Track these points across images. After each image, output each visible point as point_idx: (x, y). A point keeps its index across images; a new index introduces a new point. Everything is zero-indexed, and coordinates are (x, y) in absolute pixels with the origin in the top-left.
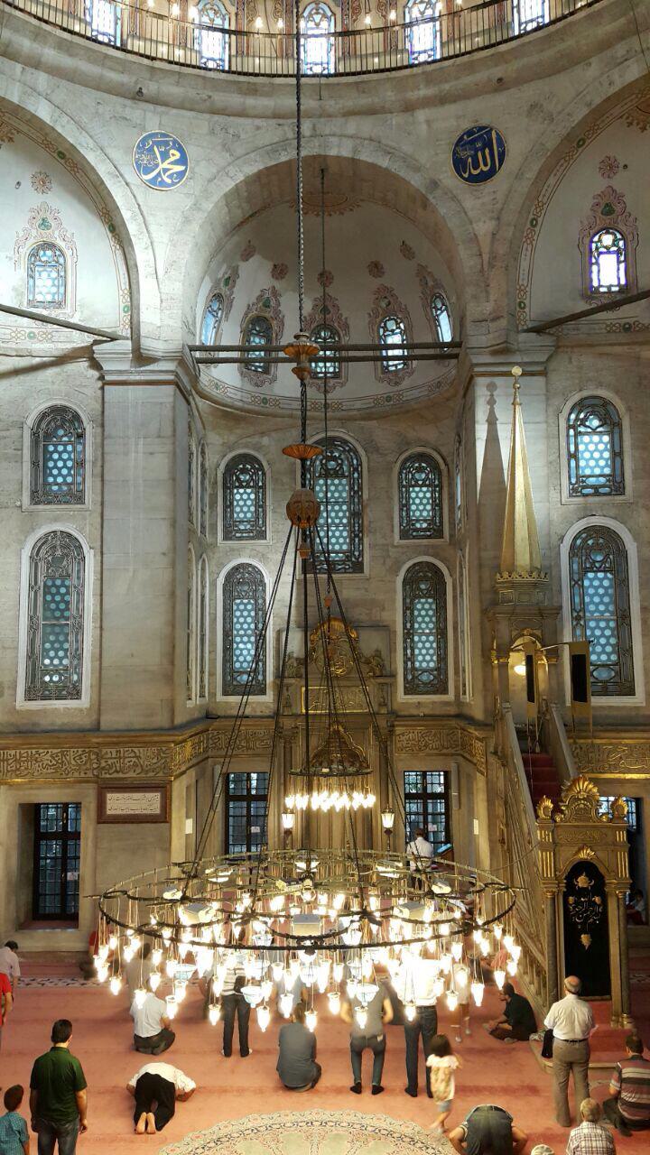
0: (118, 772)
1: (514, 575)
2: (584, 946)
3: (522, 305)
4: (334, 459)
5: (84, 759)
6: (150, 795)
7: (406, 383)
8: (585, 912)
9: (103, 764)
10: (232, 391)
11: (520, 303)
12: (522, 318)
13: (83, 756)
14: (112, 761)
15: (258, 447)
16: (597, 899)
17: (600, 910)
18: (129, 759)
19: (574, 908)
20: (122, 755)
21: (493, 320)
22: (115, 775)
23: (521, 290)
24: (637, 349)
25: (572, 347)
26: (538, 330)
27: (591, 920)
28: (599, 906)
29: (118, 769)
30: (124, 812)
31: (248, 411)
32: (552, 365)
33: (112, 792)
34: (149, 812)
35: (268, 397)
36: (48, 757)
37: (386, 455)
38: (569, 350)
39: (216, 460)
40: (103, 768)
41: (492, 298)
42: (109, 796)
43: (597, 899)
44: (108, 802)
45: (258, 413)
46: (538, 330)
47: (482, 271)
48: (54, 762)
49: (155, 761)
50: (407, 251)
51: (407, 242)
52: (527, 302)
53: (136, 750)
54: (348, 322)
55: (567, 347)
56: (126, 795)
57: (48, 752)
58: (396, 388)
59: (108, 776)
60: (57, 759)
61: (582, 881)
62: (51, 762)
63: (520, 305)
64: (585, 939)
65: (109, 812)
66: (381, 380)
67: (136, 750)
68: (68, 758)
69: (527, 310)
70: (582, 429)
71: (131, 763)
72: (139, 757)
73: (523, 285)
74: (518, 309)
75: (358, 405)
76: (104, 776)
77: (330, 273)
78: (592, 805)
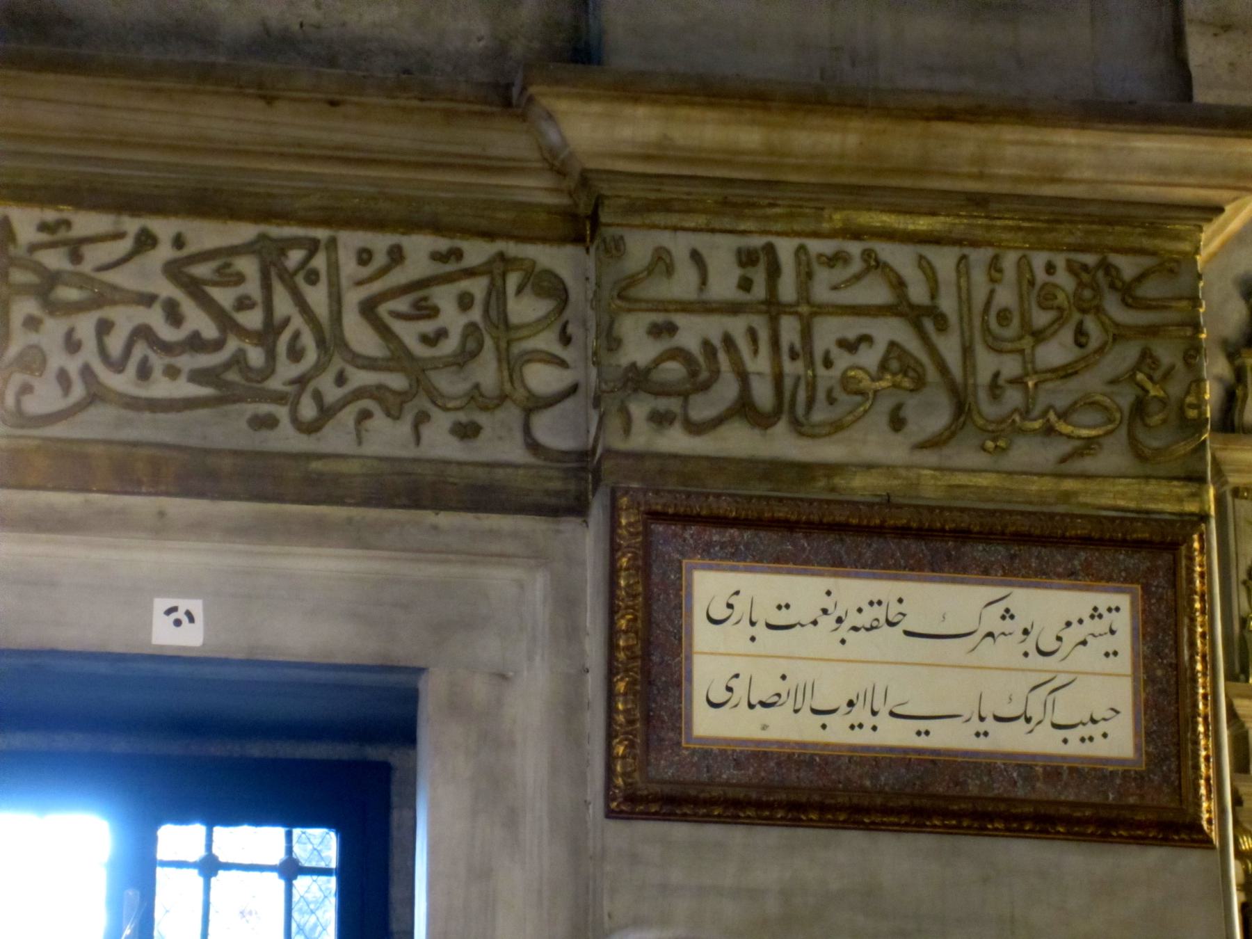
0: (761, 420)
5: (452, 319)
6: (1049, 607)
9: (638, 349)
13: (445, 297)
14: (713, 327)
18: (852, 328)
20: (787, 290)
22: (739, 441)
29: (763, 394)
30: (838, 733)
33: (736, 557)
34: (1042, 742)
36: (148, 275)
40: (638, 380)
42: (710, 587)
44: (703, 636)
48: (198, 321)
49: (1056, 352)
53: (899, 257)
56: (854, 591)
57: (146, 241)
59: (676, 441)
60: (224, 297)
62: (174, 315)
65: (707, 724)
67: (899, 257)
68: (317, 297)
71: (870, 358)
72: (922, 317)
76: (642, 438)
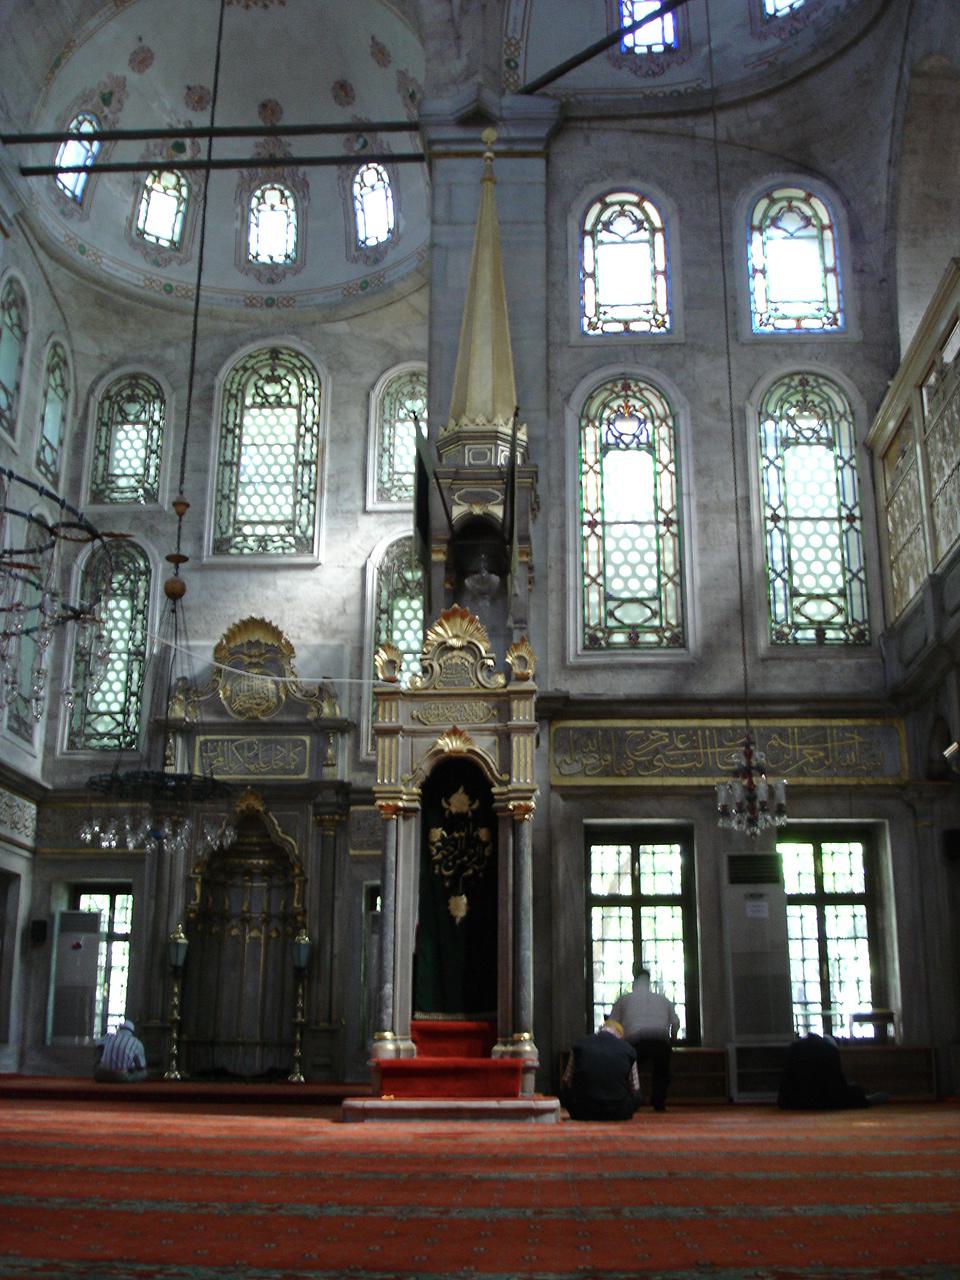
1: (464, 420)
2: (453, 919)
3: (512, 64)
4: (276, 380)
7: (390, 258)
8: (460, 856)
10: (111, 264)
11: (508, 62)
12: (511, 80)
15: (158, 364)
16: (483, 834)
17: (487, 853)
19: (439, 849)
21: (467, 78)
23: (509, 45)
24: (689, 122)
25: (591, 119)
26: (530, 90)
27: (470, 872)
28: (485, 844)
31: (141, 300)
32: (558, 147)
35: (174, 284)
37: (360, 374)
38: (585, 125)
39: (88, 383)
41: (465, 51)
43: (483, 834)
45: (153, 304)
46: (530, 90)
47: (451, 20)
50: (380, 54)
51: (379, 40)
52: (520, 61)
54: (307, 179)
55: (583, 119)
58: (377, 268)
61: (459, 802)
63: (508, 62)
64: (460, 906)
66: (355, 260)
69: (520, 71)
70: (603, 236)
73: (513, 37)
74: (505, 68)
75: (320, 299)
77: (277, 104)
78: (475, 659)
